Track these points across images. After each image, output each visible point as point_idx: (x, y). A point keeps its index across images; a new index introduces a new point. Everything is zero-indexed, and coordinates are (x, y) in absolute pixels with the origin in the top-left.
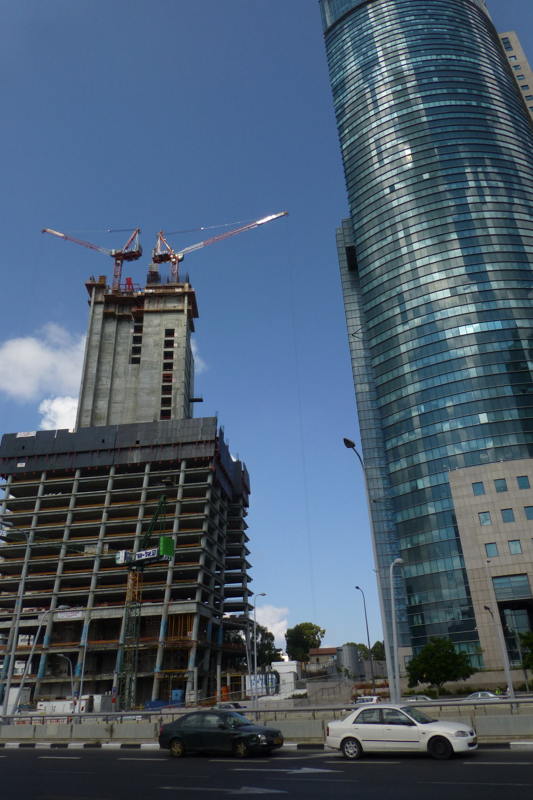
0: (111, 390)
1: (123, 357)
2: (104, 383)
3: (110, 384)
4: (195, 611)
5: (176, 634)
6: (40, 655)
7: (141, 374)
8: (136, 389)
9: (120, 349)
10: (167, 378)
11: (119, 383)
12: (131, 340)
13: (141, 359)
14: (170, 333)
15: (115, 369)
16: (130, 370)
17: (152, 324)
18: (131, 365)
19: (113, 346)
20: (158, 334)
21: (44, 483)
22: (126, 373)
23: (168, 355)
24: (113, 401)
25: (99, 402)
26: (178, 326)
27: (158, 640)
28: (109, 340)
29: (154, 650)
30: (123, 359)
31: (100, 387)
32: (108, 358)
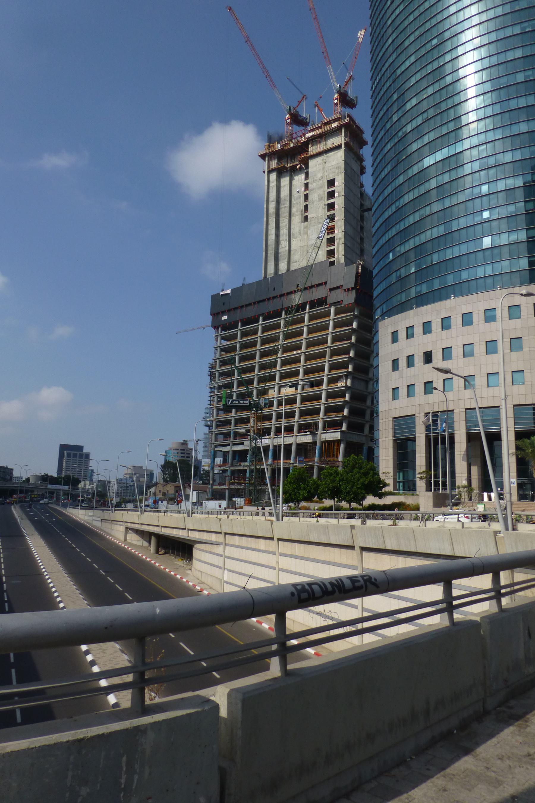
0: (289, 251)
1: (297, 217)
2: (283, 246)
3: (287, 246)
4: (339, 438)
5: (328, 456)
6: (246, 470)
8: (307, 245)
9: (294, 210)
10: (331, 230)
11: (294, 242)
12: (303, 198)
13: (309, 217)
14: (331, 183)
16: (302, 228)
17: (316, 178)
18: (302, 224)
19: (287, 209)
20: (321, 187)
21: (240, 342)
22: (300, 233)
23: (331, 207)
24: (292, 261)
25: (280, 265)
26: (338, 174)
27: (314, 461)
28: (284, 204)
29: (312, 467)
30: (297, 219)
31: (280, 250)
32: (284, 223)
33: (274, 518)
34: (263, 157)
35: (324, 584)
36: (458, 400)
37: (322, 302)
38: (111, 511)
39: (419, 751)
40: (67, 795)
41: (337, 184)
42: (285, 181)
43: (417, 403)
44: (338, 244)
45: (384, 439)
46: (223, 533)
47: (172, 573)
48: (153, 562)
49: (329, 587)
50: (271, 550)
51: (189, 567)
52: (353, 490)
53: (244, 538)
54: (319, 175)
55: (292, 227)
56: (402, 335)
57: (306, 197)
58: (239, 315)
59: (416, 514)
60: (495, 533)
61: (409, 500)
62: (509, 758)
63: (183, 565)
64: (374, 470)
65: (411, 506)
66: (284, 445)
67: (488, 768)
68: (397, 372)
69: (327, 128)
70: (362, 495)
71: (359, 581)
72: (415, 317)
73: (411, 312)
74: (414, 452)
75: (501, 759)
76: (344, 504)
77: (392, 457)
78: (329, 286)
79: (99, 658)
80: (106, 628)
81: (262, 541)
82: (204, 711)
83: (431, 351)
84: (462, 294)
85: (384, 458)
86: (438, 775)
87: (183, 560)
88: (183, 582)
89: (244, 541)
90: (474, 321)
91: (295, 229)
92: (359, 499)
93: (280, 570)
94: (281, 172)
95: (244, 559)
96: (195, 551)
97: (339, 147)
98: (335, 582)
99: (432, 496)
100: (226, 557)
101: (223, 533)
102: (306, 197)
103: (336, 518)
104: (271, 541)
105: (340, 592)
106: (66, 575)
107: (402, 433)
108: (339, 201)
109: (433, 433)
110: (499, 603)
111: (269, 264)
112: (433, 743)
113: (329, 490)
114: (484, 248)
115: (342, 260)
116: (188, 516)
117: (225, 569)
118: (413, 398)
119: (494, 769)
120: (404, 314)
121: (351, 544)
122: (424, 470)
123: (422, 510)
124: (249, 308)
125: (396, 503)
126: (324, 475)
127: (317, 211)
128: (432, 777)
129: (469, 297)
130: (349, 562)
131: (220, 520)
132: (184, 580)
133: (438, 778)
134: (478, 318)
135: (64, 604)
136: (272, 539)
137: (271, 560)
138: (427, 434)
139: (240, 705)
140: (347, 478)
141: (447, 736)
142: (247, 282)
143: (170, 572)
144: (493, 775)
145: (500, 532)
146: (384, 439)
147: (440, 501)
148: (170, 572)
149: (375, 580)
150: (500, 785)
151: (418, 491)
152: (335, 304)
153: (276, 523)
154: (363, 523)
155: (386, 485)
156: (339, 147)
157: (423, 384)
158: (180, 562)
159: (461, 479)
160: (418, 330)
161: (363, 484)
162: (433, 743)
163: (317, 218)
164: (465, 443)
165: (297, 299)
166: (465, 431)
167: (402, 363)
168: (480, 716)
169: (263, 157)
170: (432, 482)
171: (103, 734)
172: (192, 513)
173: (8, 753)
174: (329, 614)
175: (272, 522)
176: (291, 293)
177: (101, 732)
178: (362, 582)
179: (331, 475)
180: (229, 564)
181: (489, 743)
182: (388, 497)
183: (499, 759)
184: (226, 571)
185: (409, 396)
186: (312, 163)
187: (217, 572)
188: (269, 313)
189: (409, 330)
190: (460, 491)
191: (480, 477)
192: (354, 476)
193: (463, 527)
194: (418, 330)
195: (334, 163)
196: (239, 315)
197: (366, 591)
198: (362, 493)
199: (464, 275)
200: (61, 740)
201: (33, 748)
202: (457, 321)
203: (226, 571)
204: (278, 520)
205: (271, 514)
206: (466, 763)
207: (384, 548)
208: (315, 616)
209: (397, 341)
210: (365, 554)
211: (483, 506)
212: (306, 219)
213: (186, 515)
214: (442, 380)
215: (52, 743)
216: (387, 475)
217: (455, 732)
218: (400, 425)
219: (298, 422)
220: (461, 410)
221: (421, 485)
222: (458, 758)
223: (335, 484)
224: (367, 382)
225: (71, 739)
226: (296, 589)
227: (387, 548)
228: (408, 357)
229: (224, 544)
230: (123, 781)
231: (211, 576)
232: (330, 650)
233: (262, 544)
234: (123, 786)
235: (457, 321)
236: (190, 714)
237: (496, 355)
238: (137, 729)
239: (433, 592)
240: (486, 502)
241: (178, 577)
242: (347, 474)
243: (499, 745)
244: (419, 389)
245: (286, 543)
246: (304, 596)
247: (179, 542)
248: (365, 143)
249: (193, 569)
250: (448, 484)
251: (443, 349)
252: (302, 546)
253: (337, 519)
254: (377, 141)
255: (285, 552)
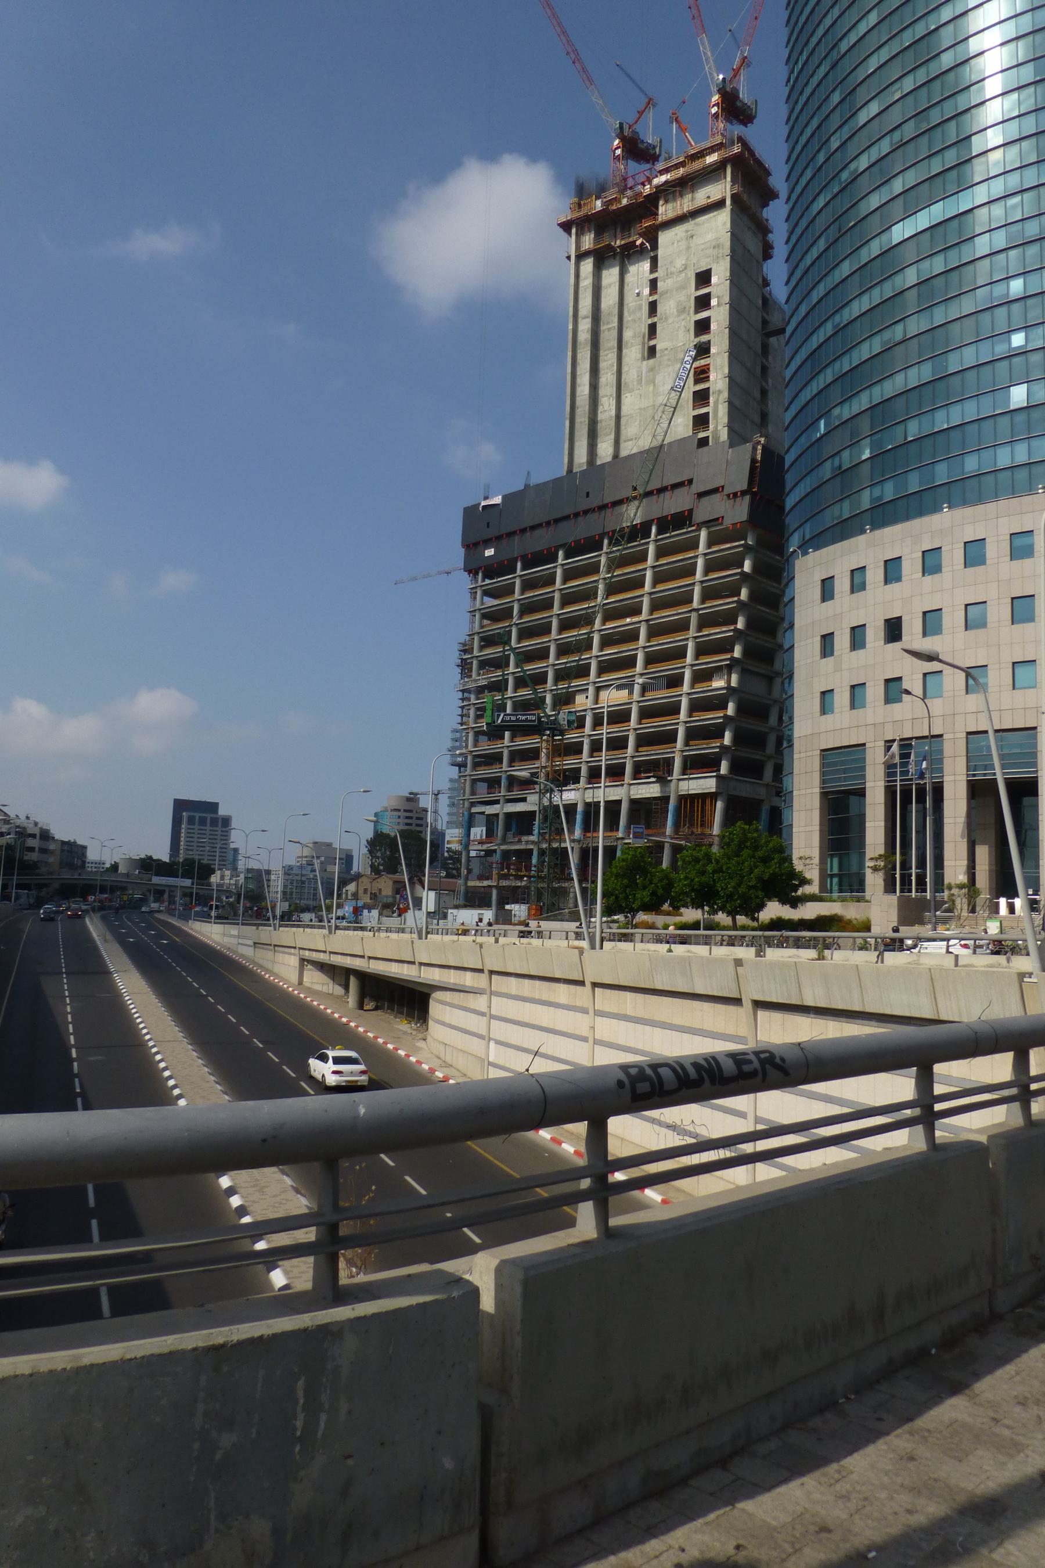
0: (618, 417)
1: (634, 349)
2: (606, 407)
4: (714, 790)
6: (531, 850)
7: (659, 379)
9: (627, 334)
10: (702, 375)
11: (627, 400)
12: (645, 308)
14: (704, 278)
15: (624, 376)
17: (673, 269)
18: (645, 363)
19: (615, 333)
20: (683, 287)
21: (519, 600)
22: (640, 382)
23: (702, 327)
24: (623, 438)
25: (599, 445)
26: (717, 259)
28: (608, 323)
29: (660, 846)
30: (633, 353)
31: (600, 417)
33: (584, 944)
34: (566, 226)
35: (682, 1067)
36: (954, 716)
37: (681, 520)
38: (272, 928)
39: (862, 1386)
40: (196, 1446)
41: (714, 280)
42: (611, 275)
43: (870, 721)
44: (716, 403)
45: (803, 792)
46: (486, 972)
47: (390, 1046)
48: (352, 1024)
49: (692, 1072)
50: (579, 1004)
51: (421, 1036)
52: (741, 890)
53: (526, 981)
54: (679, 263)
55: (625, 369)
56: (842, 585)
57: (653, 307)
58: (517, 547)
59: (864, 939)
60: (1021, 976)
61: (850, 911)
62: (1038, 1402)
63: (409, 1031)
64: (783, 854)
65: (855, 922)
66: (606, 802)
67: (996, 1420)
68: (830, 659)
69: (697, 165)
70: (758, 901)
71: (750, 1062)
72: (868, 549)
73: (862, 539)
74: (862, 818)
75: (1023, 1403)
76: (722, 918)
77: (818, 828)
78: (698, 487)
79: (254, 1202)
80: (264, 1140)
81: (563, 988)
82: (450, 1300)
83: (900, 618)
84: (965, 502)
85: (802, 829)
86: (899, 1431)
87: (410, 1022)
88: (411, 1063)
89: (527, 987)
90: (988, 555)
91: (630, 374)
92: (752, 909)
93: (596, 1042)
94: (602, 257)
95: (526, 1020)
96: (432, 1005)
97: (720, 204)
98: (703, 1063)
99: (896, 902)
100: (492, 1017)
101: (486, 972)
102: (653, 307)
103: (706, 944)
104: (579, 988)
105: (713, 1081)
106: (190, 1047)
107: (839, 779)
108: (719, 316)
109: (901, 780)
110: (1026, 1109)
111: (577, 444)
112: (889, 1371)
113: (693, 890)
114: (1012, 408)
115: (724, 435)
116: (420, 938)
117: (490, 1039)
118: (860, 711)
119: (1006, 1422)
120: (846, 543)
121: (734, 995)
122: (882, 852)
123: (875, 930)
124: (538, 532)
125: (825, 917)
126: (684, 861)
127: (677, 335)
128: (888, 1434)
129: (980, 508)
130: (731, 1030)
131: (481, 946)
132: (413, 1059)
133: (897, 1436)
134: (996, 550)
135: (187, 1100)
136: (582, 983)
137: (580, 1023)
138: (888, 781)
139: (518, 1290)
140: (729, 868)
141: (917, 1358)
142: (535, 480)
143: (385, 1043)
144: (1006, 1432)
145: (1030, 975)
146: (803, 792)
147: (912, 913)
148: (385, 1043)
149: (783, 1059)
150: (1019, 1452)
151: (868, 894)
152: (707, 524)
153: (588, 954)
154: (758, 955)
155: (805, 882)
156: (720, 204)
157: (883, 682)
158: (404, 1026)
159: (955, 871)
160: (875, 575)
161: (760, 879)
162: (889, 1371)
163: (675, 349)
164: (965, 801)
165: (633, 514)
166: (965, 777)
167: (841, 641)
168: (985, 1323)
169: (566, 226)
170: (898, 876)
171: (261, 1337)
172: (427, 933)
173: (85, 1367)
174: (690, 1128)
175: (581, 951)
176: (620, 502)
177: (257, 1334)
178: (756, 1064)
179: (697, 860)
180: (499, 1030)
181: (999, 1373)
182: (809, 904)
183: (1019, 1403)
184: (492, 1044)
185: (853, 706)
186: (665, 238)
187: (476, 1046)
188: (577, 542)
189: (856, 575)
190: (953, 895)
191: (994, 867)
192: (743, 863)
193: (956, 965)
194: (875, 575)
195: (710, 237)
196: (517, 547)
197: (764, 1080)
198: (757, 897)
199: (971, 464)
200: (180, 1347)
201: (131, 1359)
202: (953, 556)
203: (492, 1044)
204: (593, 947)
205: (579, 936)
206: (953, 1409)
207: (799, 1003)
208: (664, 1131)
209: (832, 598)
210: (761, 1014)
211: (998, 924)
212: (652, 352)
213: (415, 936)
214: (921, 676)
215: (166, 1350)
216: (808, 861)
217: (933, 1351)
218: (835, 764)
219: (633, 757)
220: (958, 735)
221: (874, 881)
222: (937, 1400)
223: (704, 879)
224: (770, 680)
225: (201, 1344)
226: (628, 1075)
227: (806, 1004)
228: (853, 629)
229: (488, 992)
230: (299, 1424)
231: (464, 1052)
232: (691, 1195)
233: (562, 993)
234: (298, 1433)
235: (953, 556)
236: (425, 1303)
237: (1032, 624)
238: (324, 1330)
239: (896, 1087)
240: (1005, 917)
241: (402, 1053)
242: (729, 859)
243: (1018, 1378)
244: (875, 692)
245: (608, 992)
246: (643, 1087)
247: (403, 987)
248: (773, 195)
249: (429, 1039)
250: (928, 880)
251: (925, 613)
252: (640, 997)
253: (708, 947)
254: (799, 147)
255: (607, 1008)
